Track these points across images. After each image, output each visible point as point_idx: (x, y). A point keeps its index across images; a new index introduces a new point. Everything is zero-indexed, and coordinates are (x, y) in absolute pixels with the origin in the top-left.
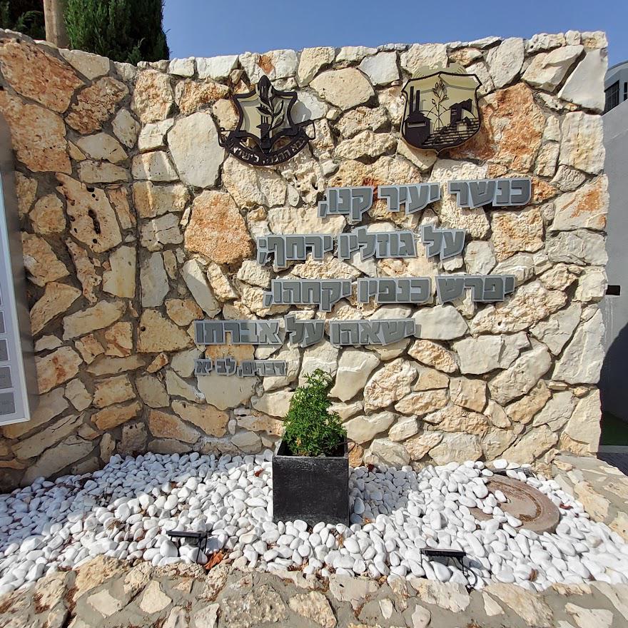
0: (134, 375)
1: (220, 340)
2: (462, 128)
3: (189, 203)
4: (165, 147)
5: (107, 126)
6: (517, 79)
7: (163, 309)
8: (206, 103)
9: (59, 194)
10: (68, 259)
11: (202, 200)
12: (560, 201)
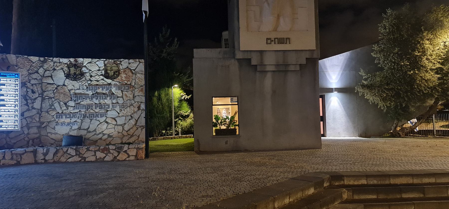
1: (62, 118)
2: (115, 76)
3: (56, 88)
4: (51, 77)
6: (127, 67)
9: (26, 87)
10: (26, 100)
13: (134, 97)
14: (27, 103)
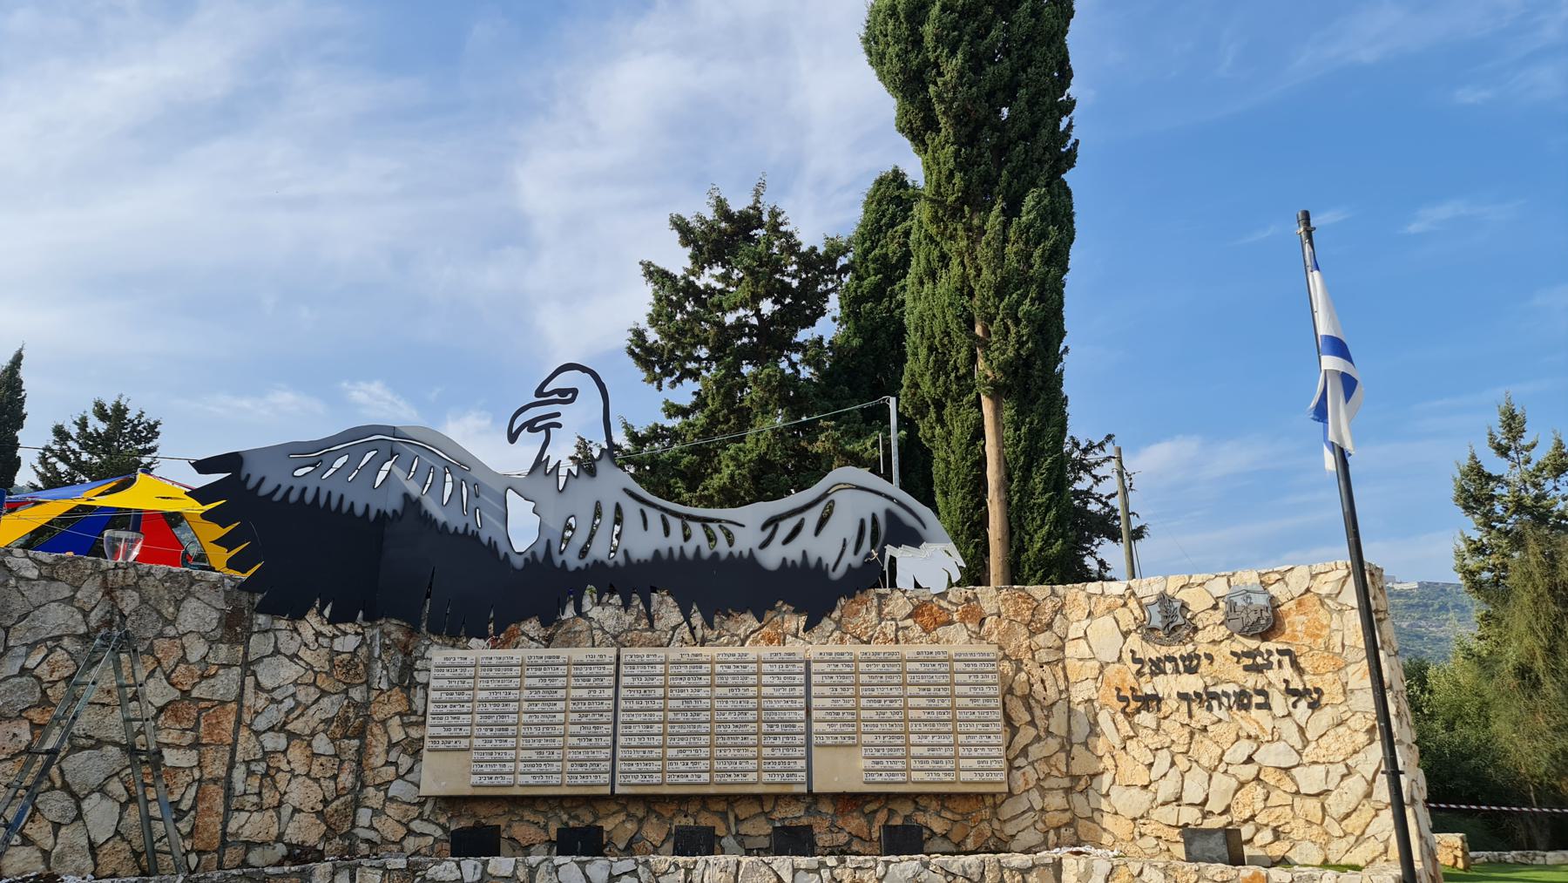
0: (1068, 791)
5: (1049, 626)
6: (1308, 590)
7: (1086, 744)
8: (1110, 610)
10: (1030, 709)
11: (1108, 671)
12: (1350, 670)
14: (1032, 715)
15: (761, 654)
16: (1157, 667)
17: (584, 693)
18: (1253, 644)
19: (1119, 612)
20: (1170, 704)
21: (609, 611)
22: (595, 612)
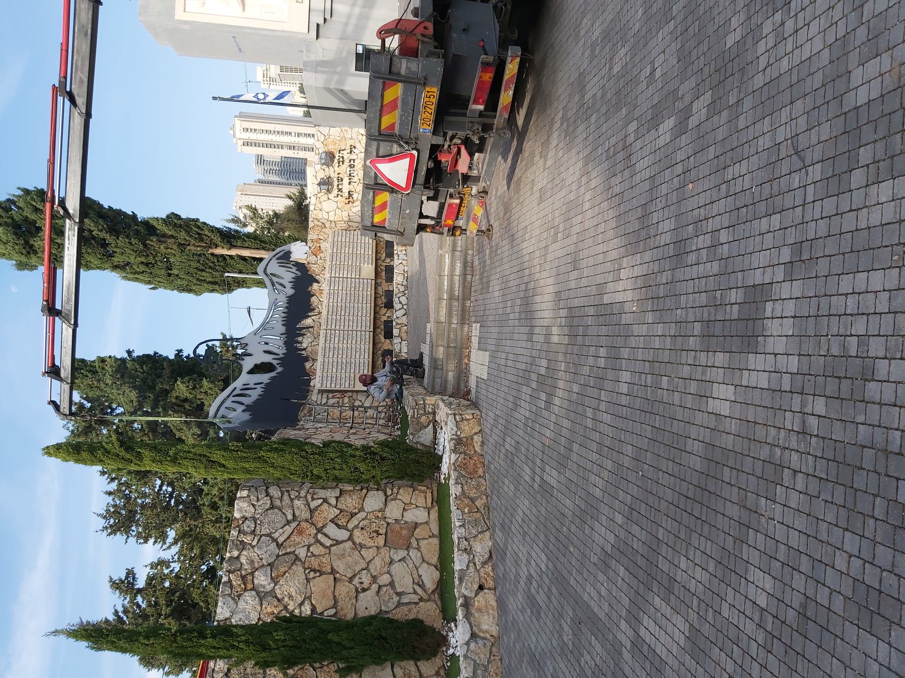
8: (320, 203)
13: (351, 138)
15: (323, 296)
16: (340, 190)
17: (337, 339)
18: (336, 161)
19: (322, 200)
20: (351, 188)
21: (304, 340)
22: (304, 345)
